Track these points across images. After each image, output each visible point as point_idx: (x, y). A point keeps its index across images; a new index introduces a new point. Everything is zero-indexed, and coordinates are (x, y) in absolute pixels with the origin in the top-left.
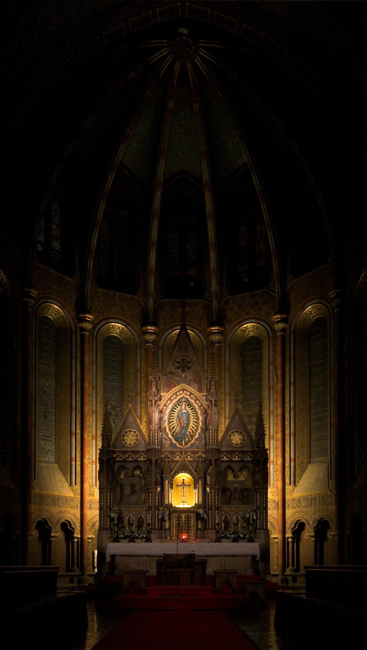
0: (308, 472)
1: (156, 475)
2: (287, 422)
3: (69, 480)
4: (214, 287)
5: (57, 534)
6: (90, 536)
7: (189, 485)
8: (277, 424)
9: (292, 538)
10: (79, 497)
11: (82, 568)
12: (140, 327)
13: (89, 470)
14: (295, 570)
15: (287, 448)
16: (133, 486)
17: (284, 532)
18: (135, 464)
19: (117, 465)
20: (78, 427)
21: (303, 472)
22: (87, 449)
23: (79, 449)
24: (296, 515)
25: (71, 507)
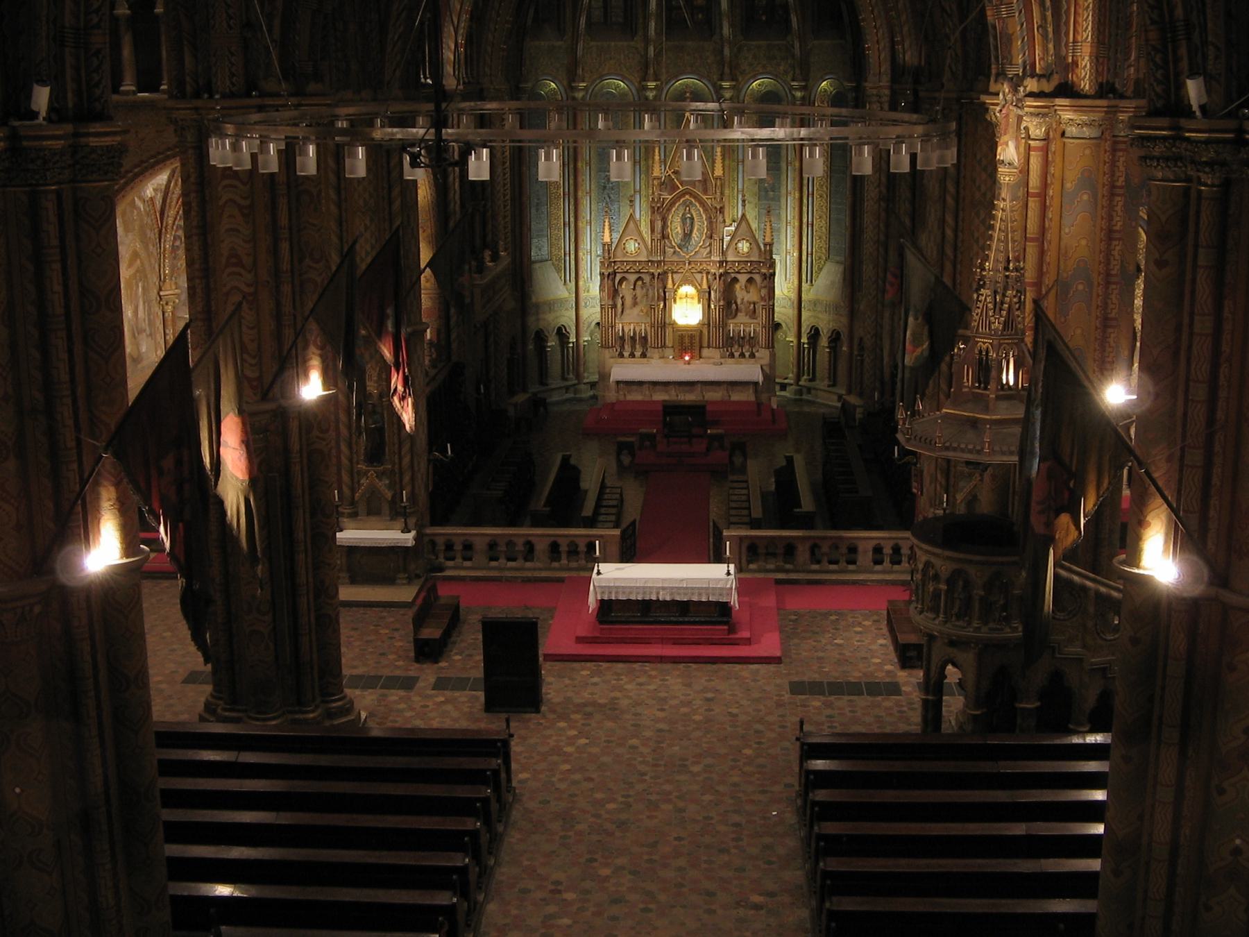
0: (825, 271)
1: (658, 291)
2: (805, 209)
3: (563, 278)
4: (726, 30)
5: (552, 342)
6: (586, 339)
7: (692, 298)
8: (794, 208)
9: (808, 344)
10: (574, 295)
11: (578, 376)
12: (638, 80)
13: (584, 262)
14: (810, 380)
15: (804, 239)
16: (635, 297)
17: (799, 336)
18: (636, 276)
19: (618, 277)
20: (572, 214)
21: (820, 269)
22: (581, 208)
23: (573, 240)
24: (812, 319)
25: (567, 309)
